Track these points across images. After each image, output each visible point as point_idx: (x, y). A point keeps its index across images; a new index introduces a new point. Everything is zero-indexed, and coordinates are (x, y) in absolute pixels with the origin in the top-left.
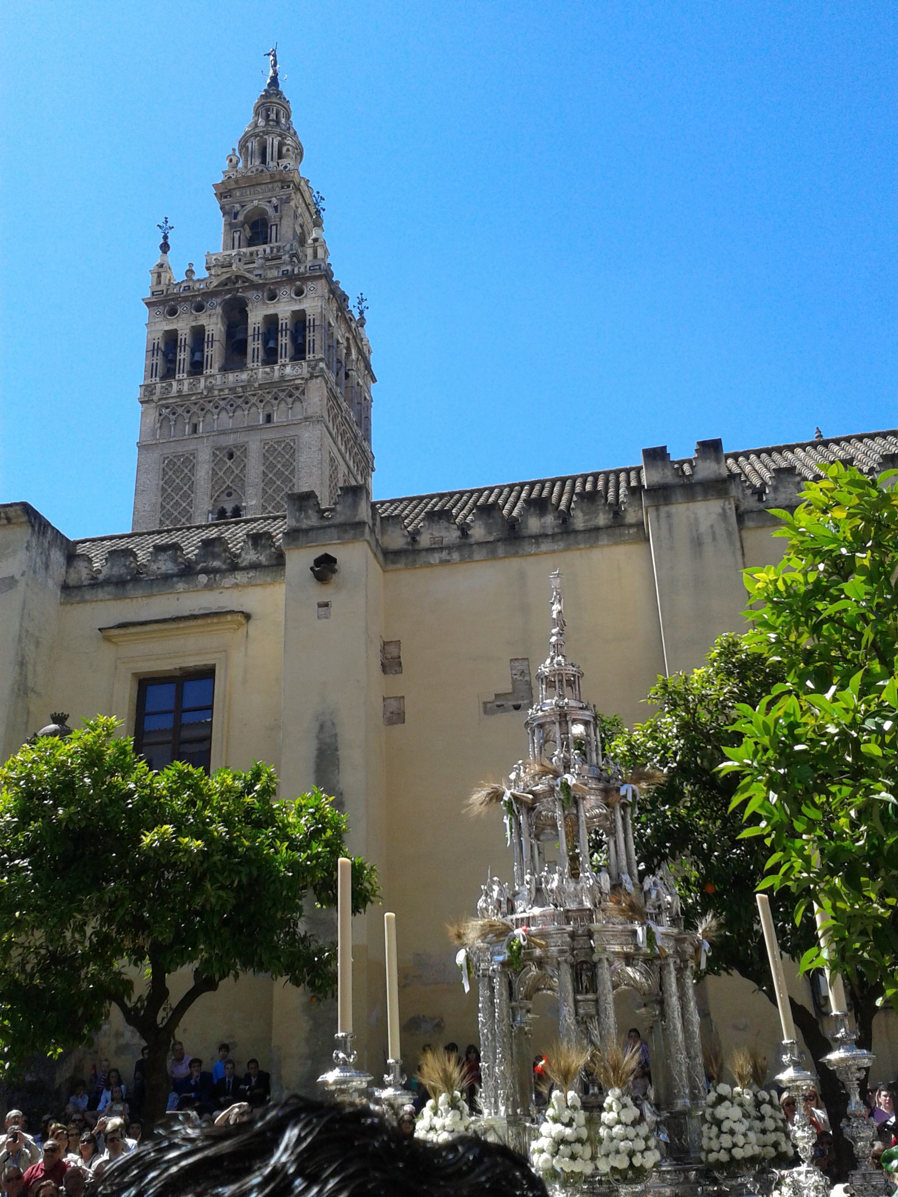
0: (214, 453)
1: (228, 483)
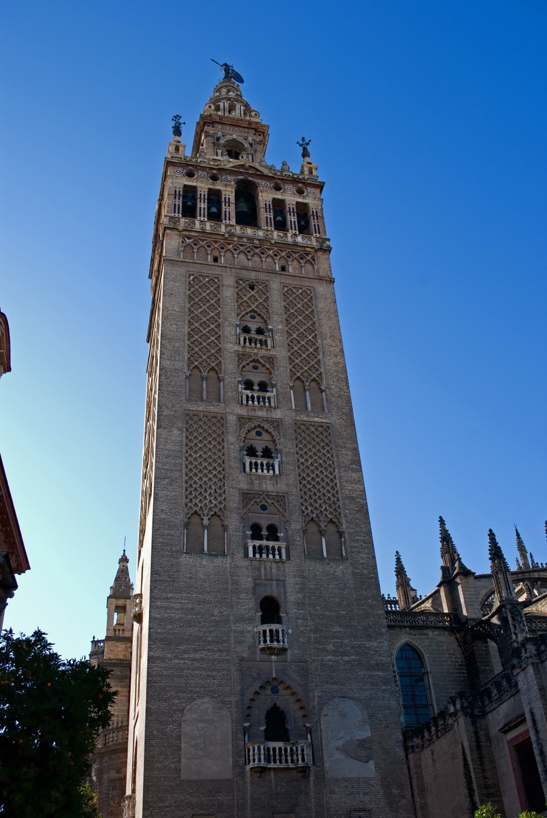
1: (253, 307)
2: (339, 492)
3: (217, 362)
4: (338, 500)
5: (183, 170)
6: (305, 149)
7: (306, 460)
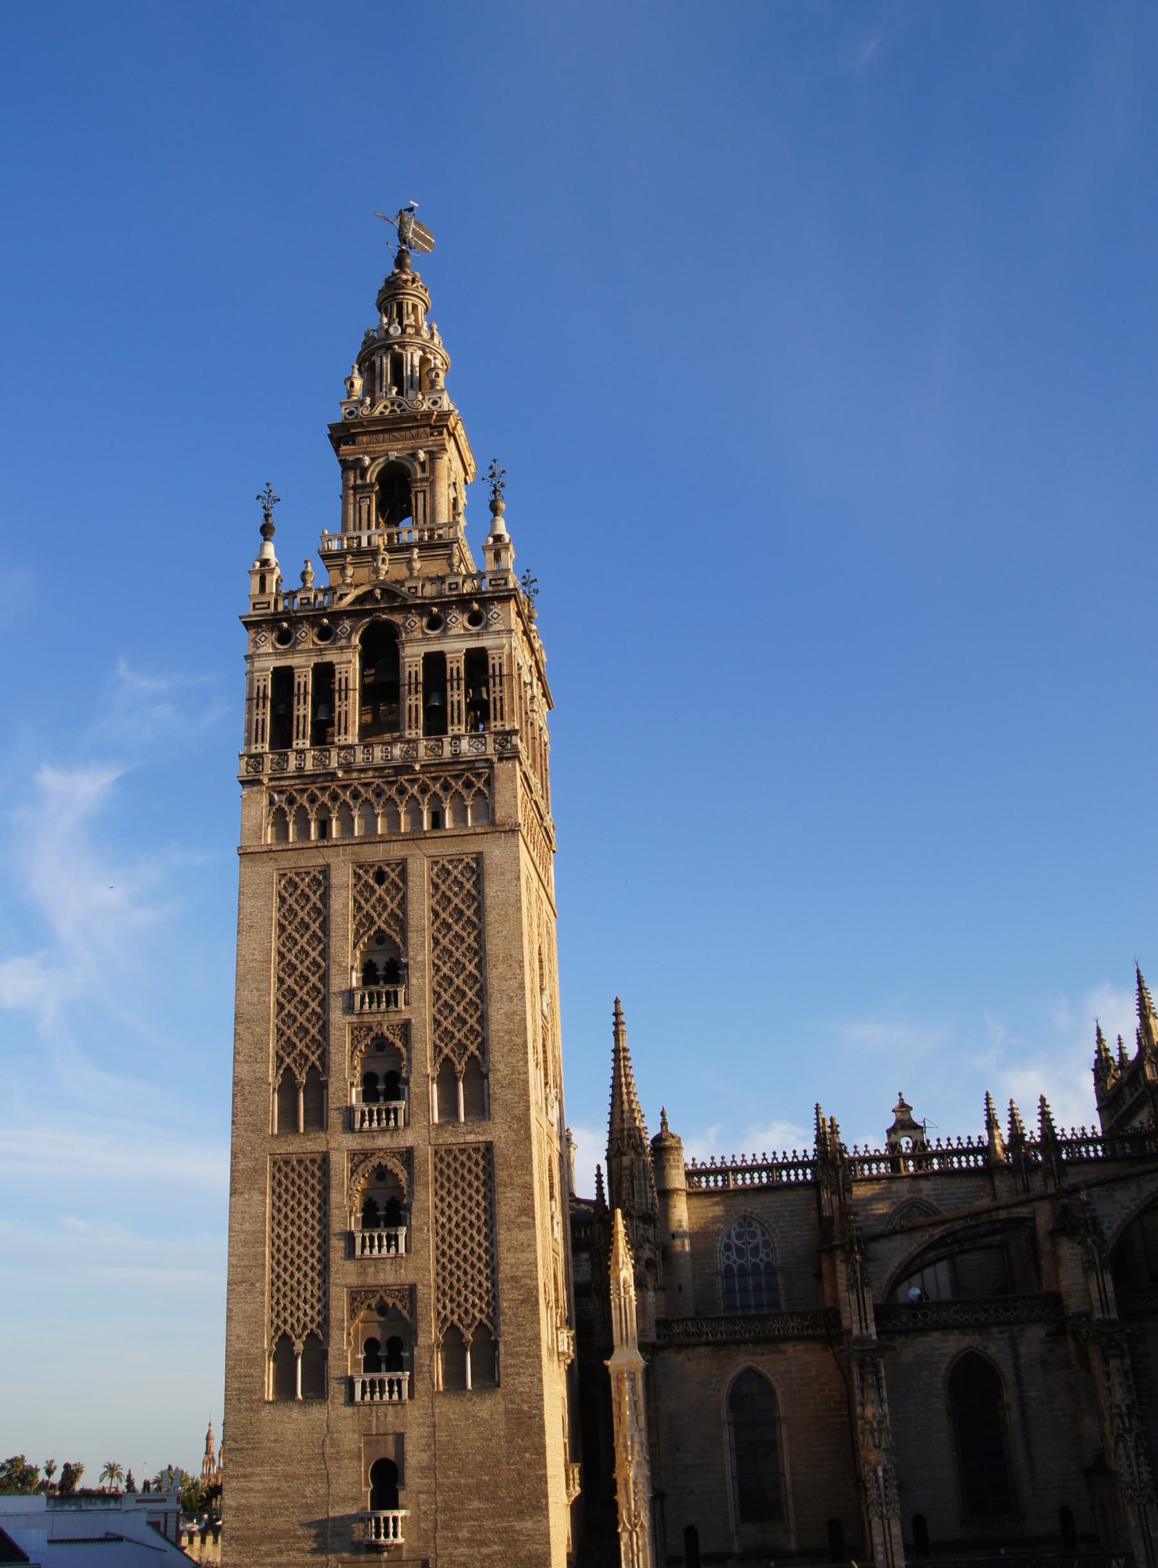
0: (355, 873)
7: (450, 1219)
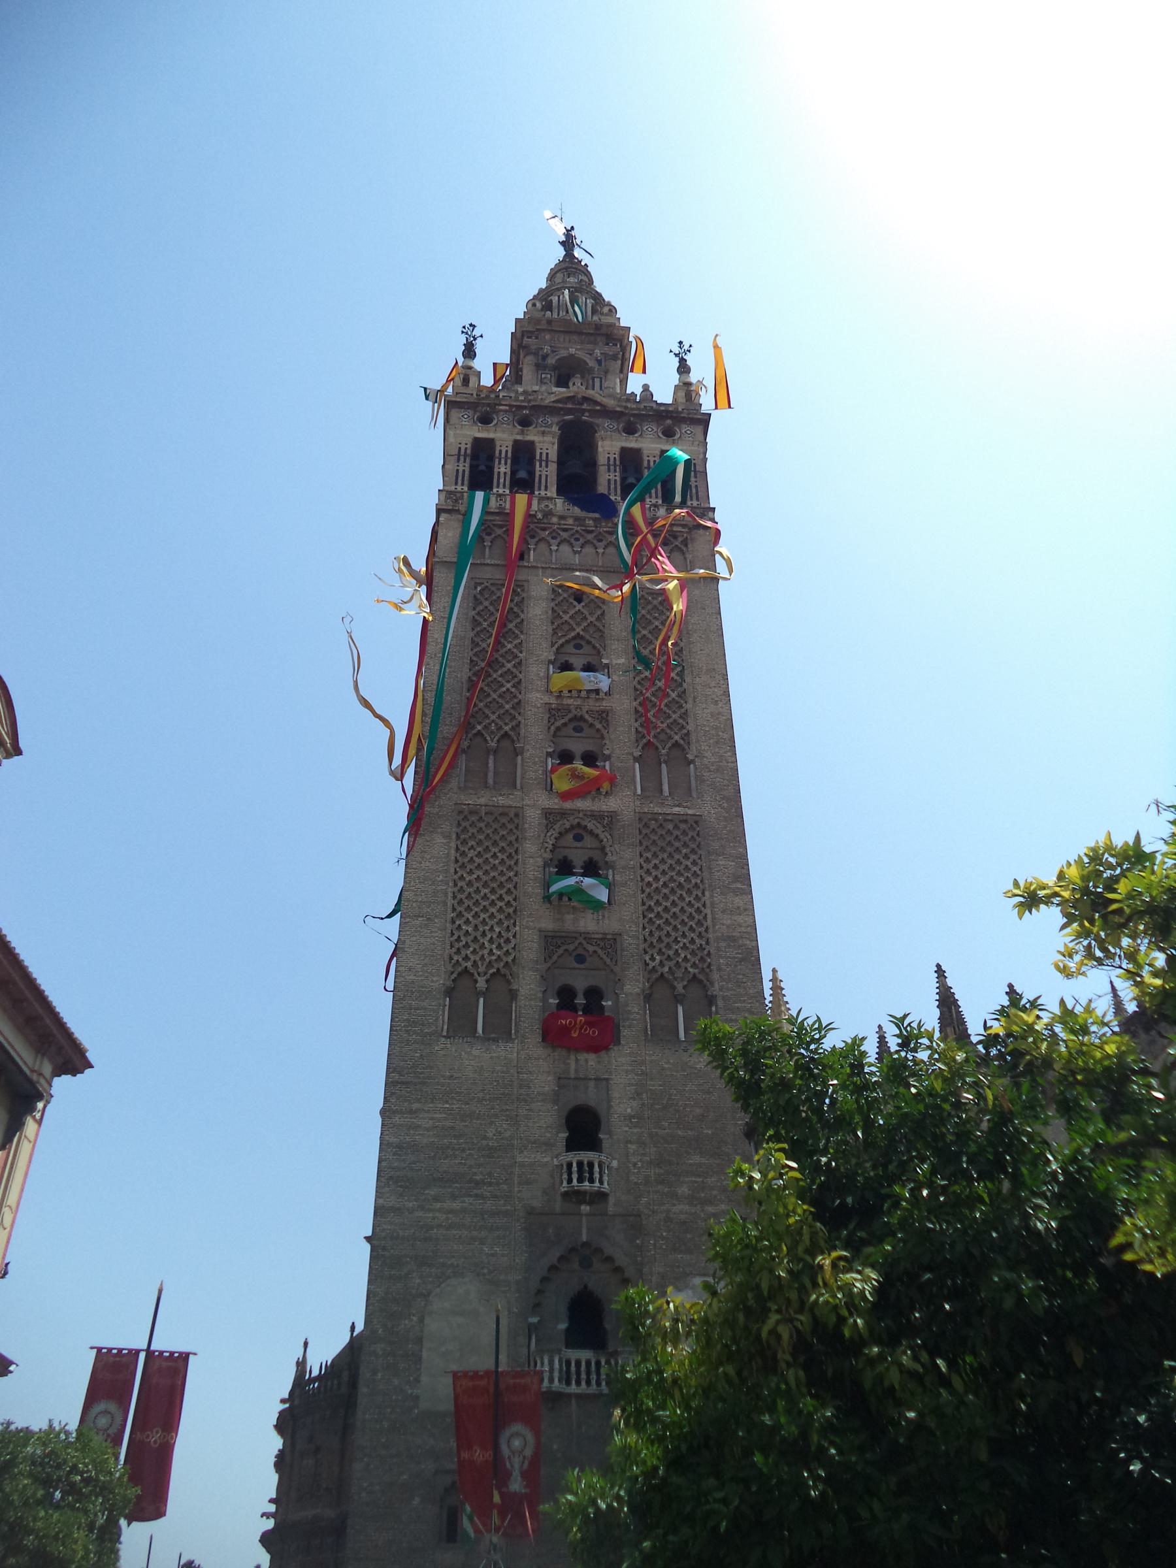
2: (711, 930)
3: (514, 723)
4: (707, 943)
5: (475, 412)
6: (683, 361)
7: (656, 879)
